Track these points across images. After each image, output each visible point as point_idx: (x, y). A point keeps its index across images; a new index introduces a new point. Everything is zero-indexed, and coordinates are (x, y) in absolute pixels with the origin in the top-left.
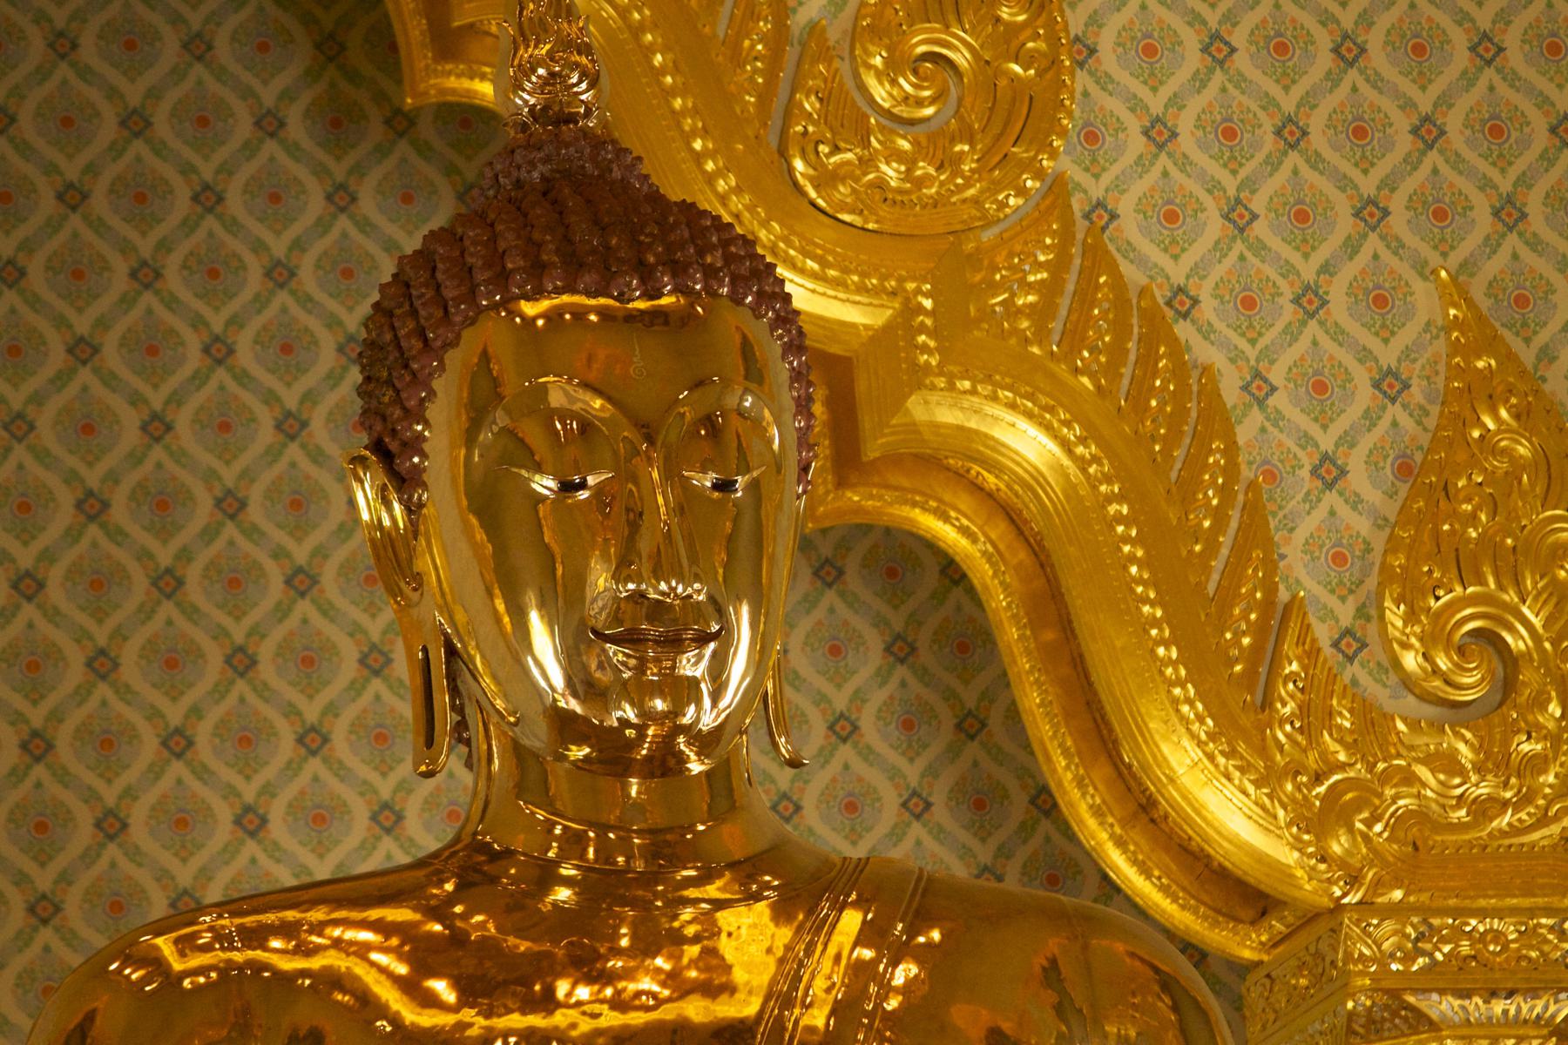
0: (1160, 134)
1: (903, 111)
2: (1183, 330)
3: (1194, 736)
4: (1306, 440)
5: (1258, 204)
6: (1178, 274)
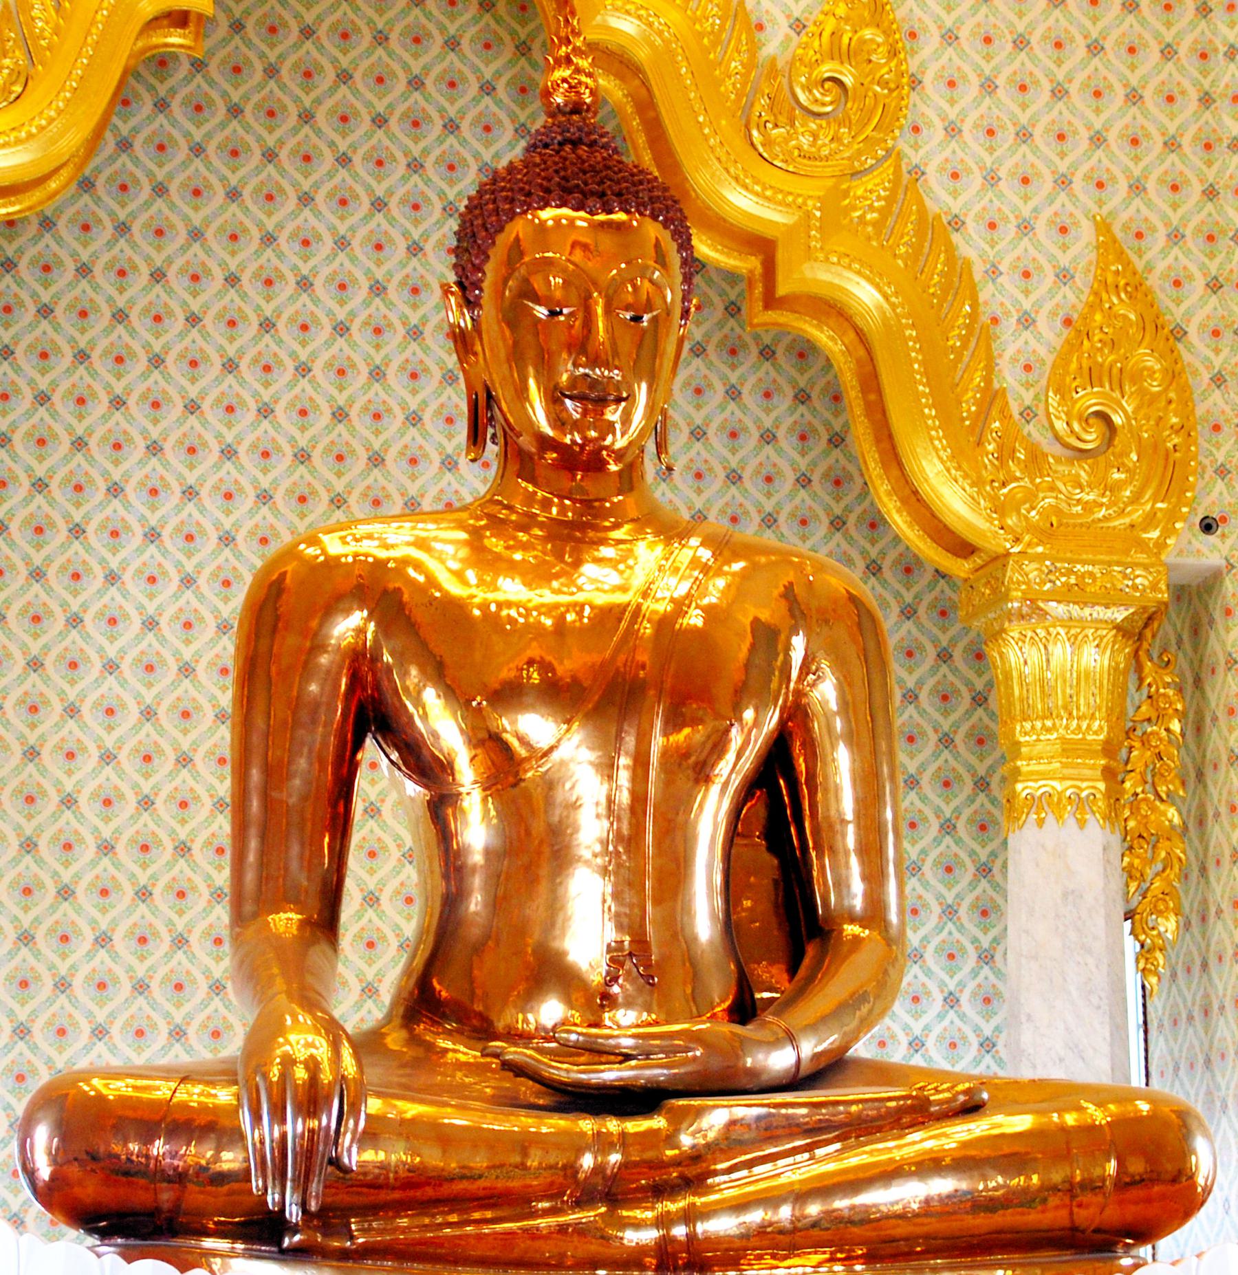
1: (816, 109)
2: (956, 238)
3: (940, 458)
6: (956, 207)
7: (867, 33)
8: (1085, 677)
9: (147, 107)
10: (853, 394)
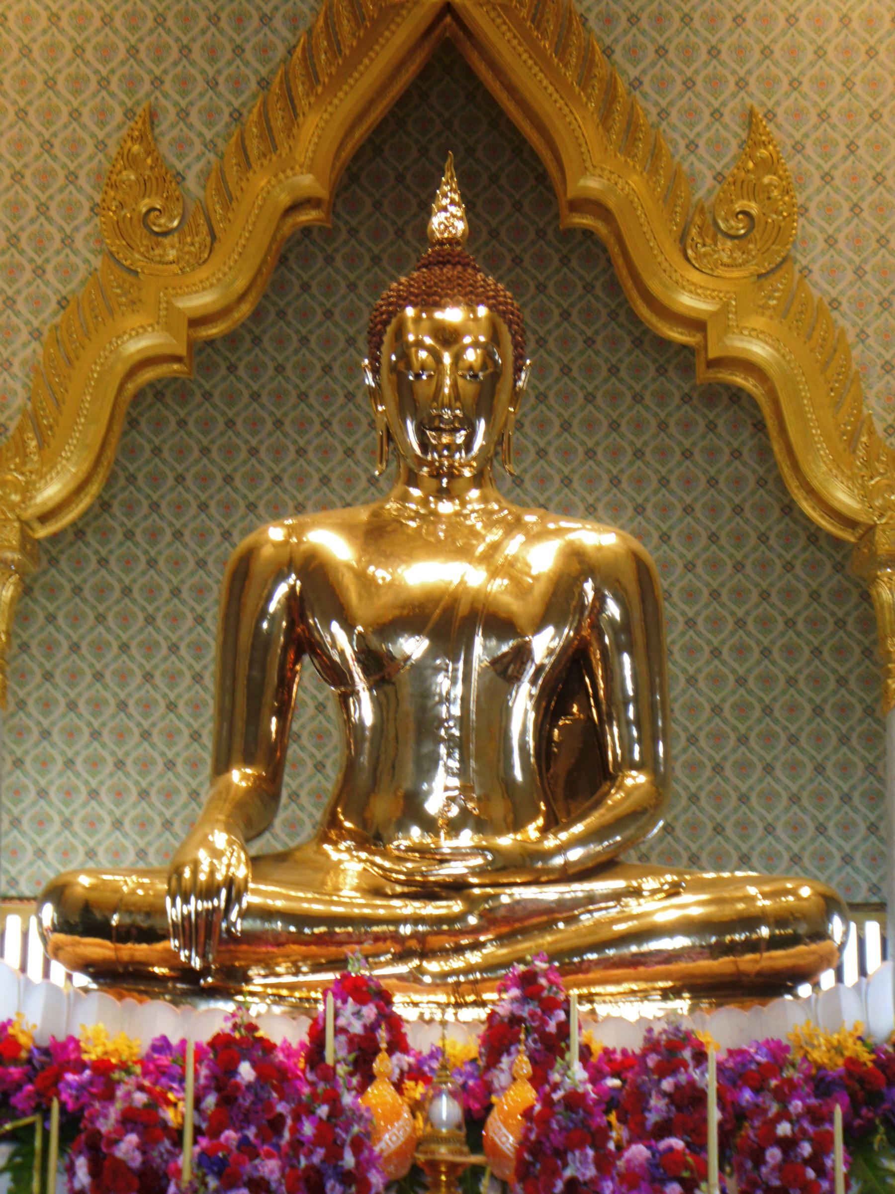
0: (831, 241)
1: (732, 232)
7: (766, 180)
9: (320, 262)
10: (771, 423)
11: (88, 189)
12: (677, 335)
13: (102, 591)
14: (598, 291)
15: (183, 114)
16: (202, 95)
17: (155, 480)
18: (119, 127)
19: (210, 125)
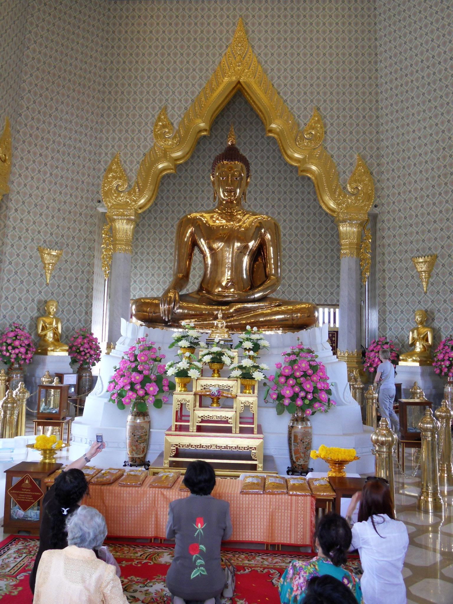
0: (332, 140)
4: (342, 169)
5: (341, 147)
7: (316, 125)
8: (354, 232)
11: (151, 127)
12: (295, 164)
13: (155, 225)
14: (276, 152)
15: (173, 108)
16: (178, 103)
17: (168, 198)
18: (158, 111)
19: (180, 111)
